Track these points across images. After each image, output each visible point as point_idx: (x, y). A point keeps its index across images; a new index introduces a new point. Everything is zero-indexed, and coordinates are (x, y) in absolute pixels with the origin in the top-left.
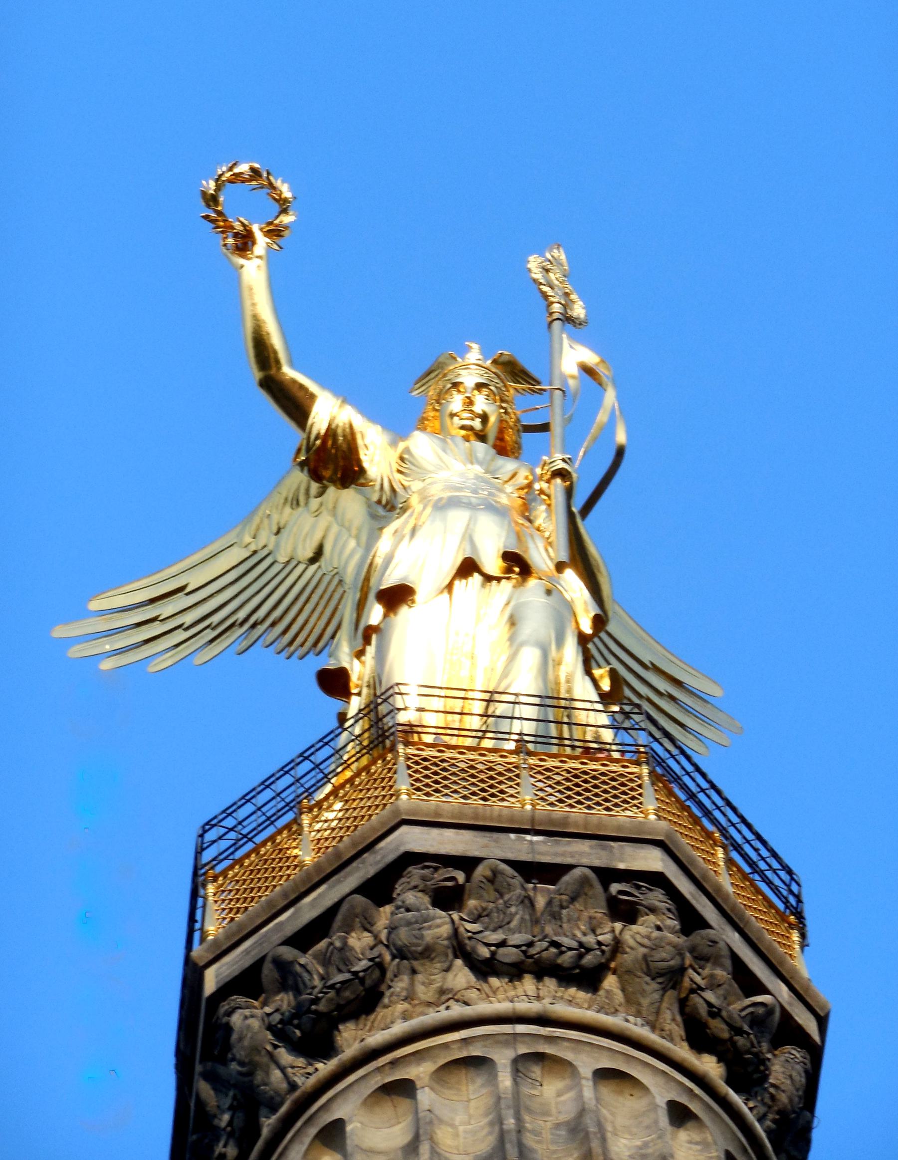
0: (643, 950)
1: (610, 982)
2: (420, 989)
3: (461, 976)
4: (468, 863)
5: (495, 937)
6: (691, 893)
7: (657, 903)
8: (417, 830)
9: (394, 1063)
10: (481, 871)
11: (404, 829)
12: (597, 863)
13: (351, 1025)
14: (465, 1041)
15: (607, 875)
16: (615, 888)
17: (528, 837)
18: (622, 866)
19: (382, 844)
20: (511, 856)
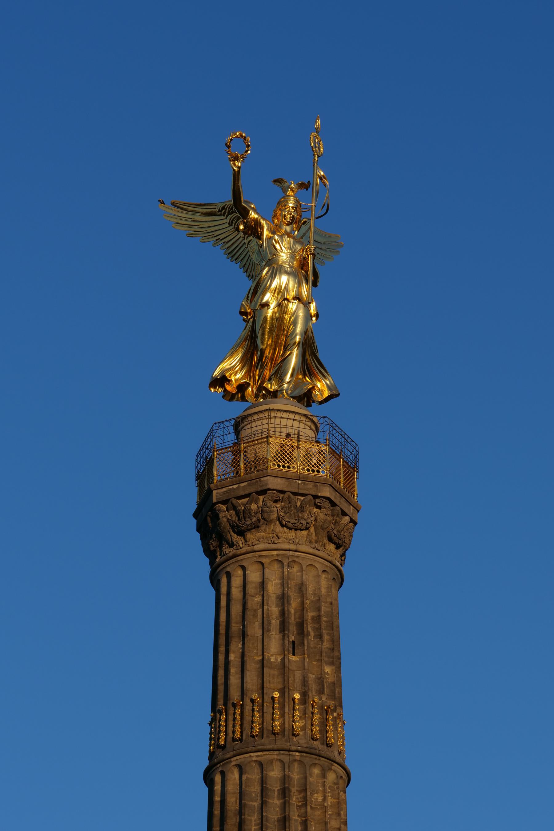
0: (322, 523)
1: (312, 529)
2: (268, 530)
3: (278, 528)
4: (283, 492)
5: (287, 520)
6: (335, 498)
7: (326, 506)
8: (272, 478)
9: (259, 556)
10: (286, 495)
11: (268, 477)
12: (314, 493)
13: (249, 534)
14: (277, 555)
15: (315, 497)
16: (317, 500)
17: (298, 481)
18: (319, 494)
19: (262, 479)
20: (294, 490)
